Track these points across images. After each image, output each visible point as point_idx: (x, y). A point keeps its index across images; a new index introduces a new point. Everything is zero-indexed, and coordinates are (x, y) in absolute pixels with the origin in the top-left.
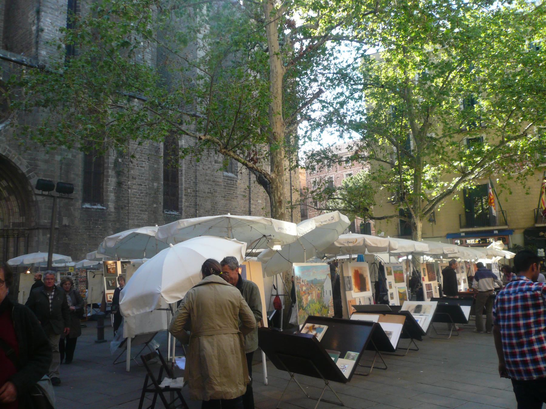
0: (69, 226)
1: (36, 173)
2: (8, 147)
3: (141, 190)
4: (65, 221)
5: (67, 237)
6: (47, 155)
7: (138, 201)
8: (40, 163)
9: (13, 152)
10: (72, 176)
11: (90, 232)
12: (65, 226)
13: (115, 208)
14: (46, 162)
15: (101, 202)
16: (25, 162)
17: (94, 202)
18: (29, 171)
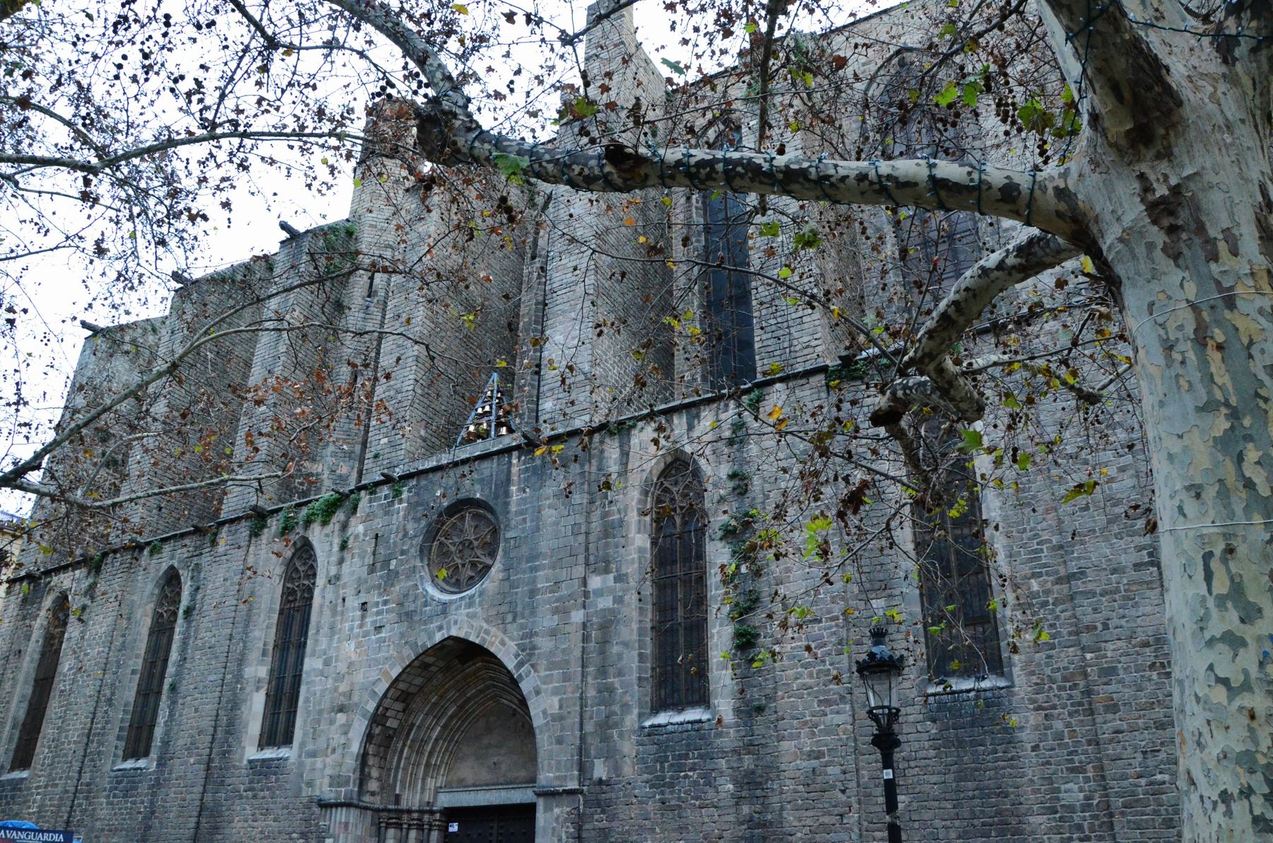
0: (608, 783)
1: (533, 666)
2: (485, 626)
3: (822, 637)
4: (600, 770)
5: (603, 812)
6: (556, 617)
7: (811, 676)
8: (538, 641)
9: (493, 630)
10: (615, 649)
11: (662, 793)
12: (600, 782)
13: (737, 711)
14: (553, 633)
15: (702, 698)
16: (512, 646)
17: (679, 707)
18: (520, 665)
